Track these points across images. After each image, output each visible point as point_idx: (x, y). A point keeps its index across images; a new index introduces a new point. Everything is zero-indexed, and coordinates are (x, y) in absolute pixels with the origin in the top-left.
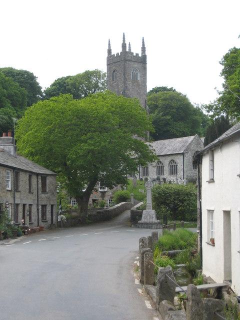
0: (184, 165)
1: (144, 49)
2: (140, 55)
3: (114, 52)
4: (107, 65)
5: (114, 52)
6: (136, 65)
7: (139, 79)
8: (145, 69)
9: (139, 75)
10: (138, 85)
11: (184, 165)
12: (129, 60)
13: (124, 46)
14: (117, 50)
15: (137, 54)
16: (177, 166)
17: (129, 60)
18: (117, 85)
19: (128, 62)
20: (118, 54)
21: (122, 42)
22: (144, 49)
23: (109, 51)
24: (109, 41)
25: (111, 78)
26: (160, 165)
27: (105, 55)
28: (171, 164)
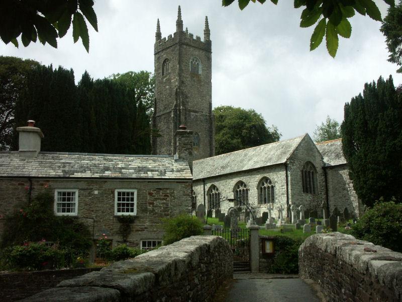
0: (287, 185)
1: (207, 32)
2: (202, 40)
3: (165, 35)
4: (155, 54)
5: (165, 35)
6: (197, 53)
7: (200, 72)
8: (209, 59)
9: (200, 67)
10: (199, 81)
11: (287, 185)
12: (187, 45)
13: (180, 23)
14: (169, 30)
15: (198, 38)
16: (273, 187)
17: (187, 45)
18: (169, 80)
19: (185, 46)
20: (171, 35)
21: (177, 18)
22: (207, 32)
23: (158, 35)
24: (158, 22)
25: (161, 71)
26: (241, 188)
27: (153, 40)
28: (261, 185)
